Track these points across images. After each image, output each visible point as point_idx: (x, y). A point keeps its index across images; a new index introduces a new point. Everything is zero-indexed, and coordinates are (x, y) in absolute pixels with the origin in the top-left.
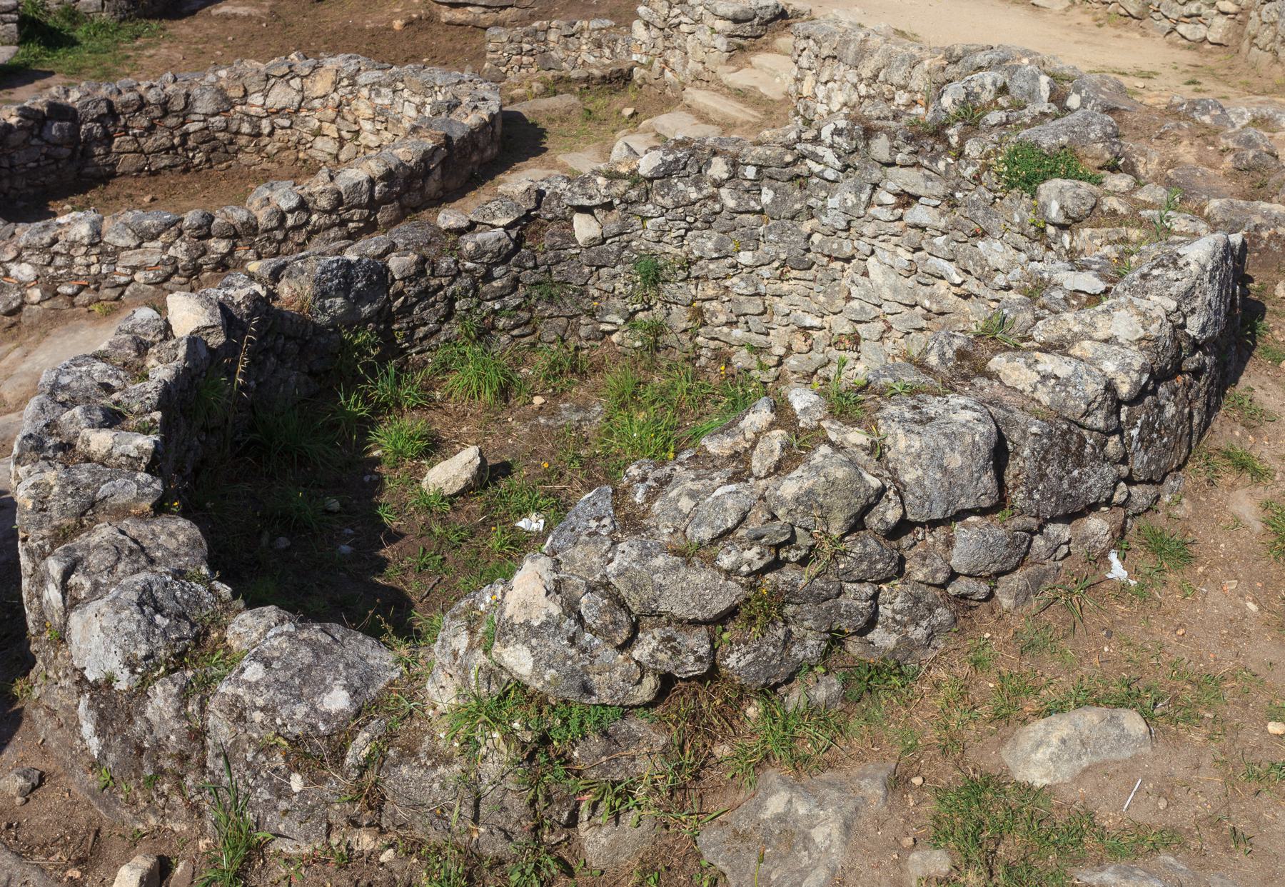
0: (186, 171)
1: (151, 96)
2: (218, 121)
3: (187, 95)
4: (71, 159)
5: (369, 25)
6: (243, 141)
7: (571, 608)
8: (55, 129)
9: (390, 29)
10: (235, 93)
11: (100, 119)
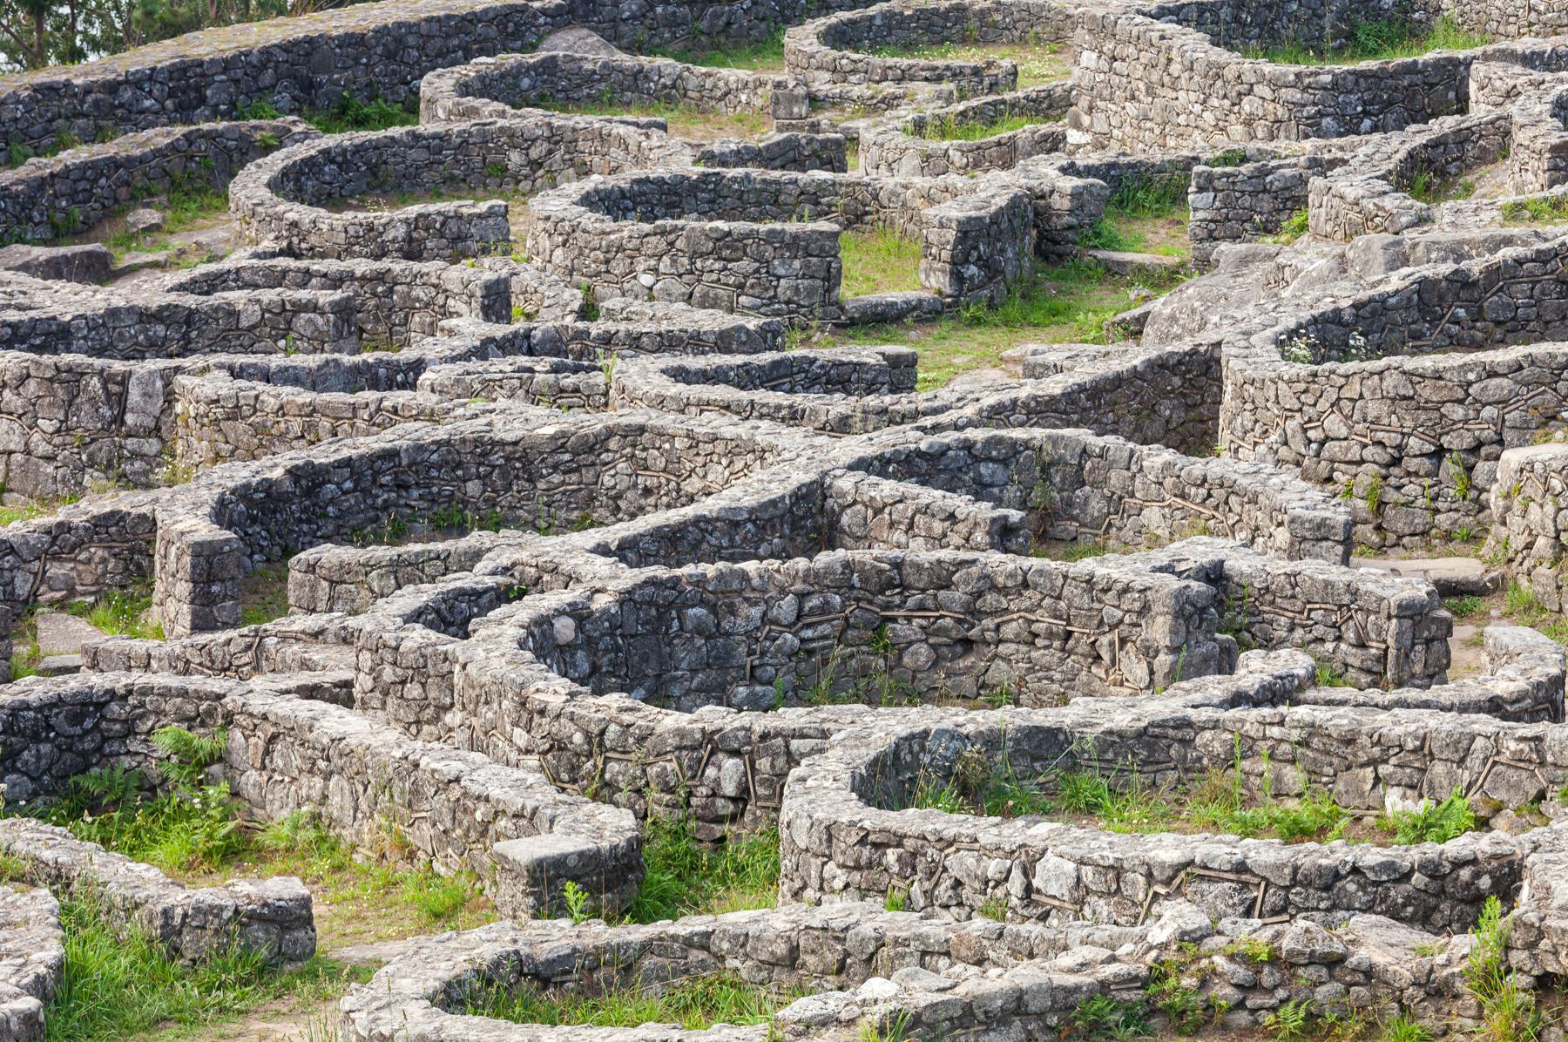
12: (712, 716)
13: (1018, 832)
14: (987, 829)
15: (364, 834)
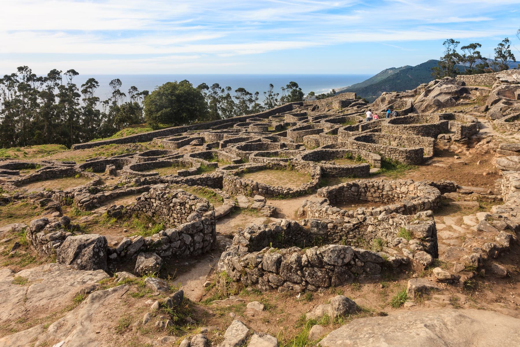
0: (383, 203)
1: (375, 185)
2: (390, 193)
3: (383, 185)
4: (357, 195)
5: (476, 173)
6: (396, 198)
7: (229, 263)
8: (353, 189)
9: (482, 175)
10: (394, 187)
11: (364, 188)
12: (247, 152)
13: (263, 158)
14: (261, 158)
15: (225, 160)
